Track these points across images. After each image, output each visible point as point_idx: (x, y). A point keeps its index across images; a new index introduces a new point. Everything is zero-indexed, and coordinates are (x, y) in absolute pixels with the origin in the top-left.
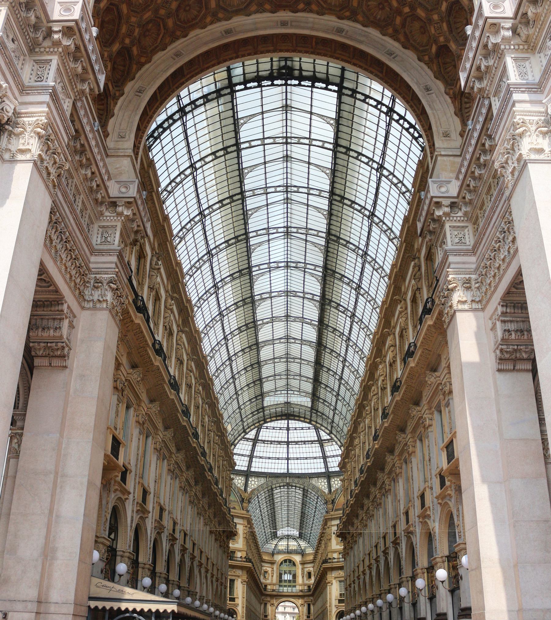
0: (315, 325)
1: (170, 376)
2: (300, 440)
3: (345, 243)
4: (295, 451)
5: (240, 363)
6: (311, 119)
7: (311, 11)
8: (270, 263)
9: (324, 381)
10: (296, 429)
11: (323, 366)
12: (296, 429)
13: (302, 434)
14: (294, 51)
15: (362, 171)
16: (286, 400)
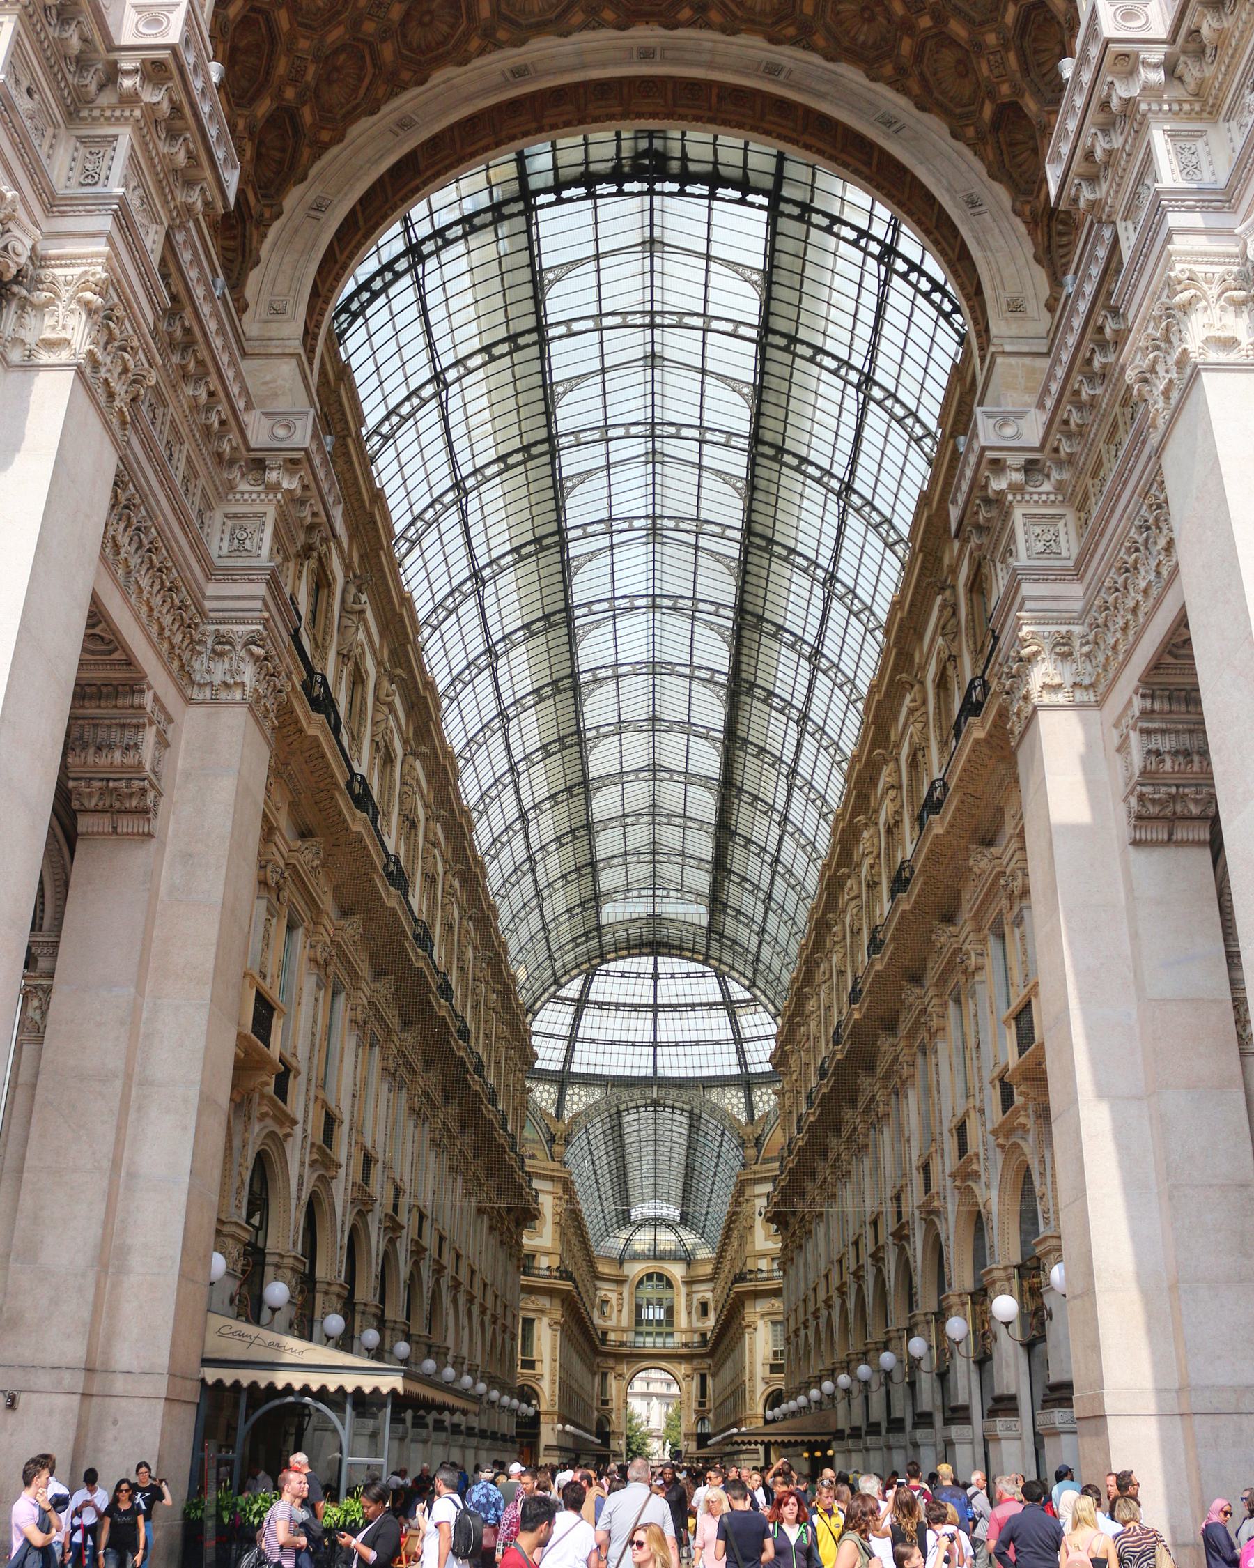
0: (716, 740)
1: (388, 855)
2: (682, 1000)
3: (784, 552)
4: (670, 1026)
5: (545, 827)
6: (707, 271)
7: (708, 25)
8: (614, 598)
9: (736, 867)
10: (673, 976)
11: (735, 833)
12: (673, 976)
13: (687, 988)
14: (669, 116)
15: (823, 389)
16: (650, 911)
